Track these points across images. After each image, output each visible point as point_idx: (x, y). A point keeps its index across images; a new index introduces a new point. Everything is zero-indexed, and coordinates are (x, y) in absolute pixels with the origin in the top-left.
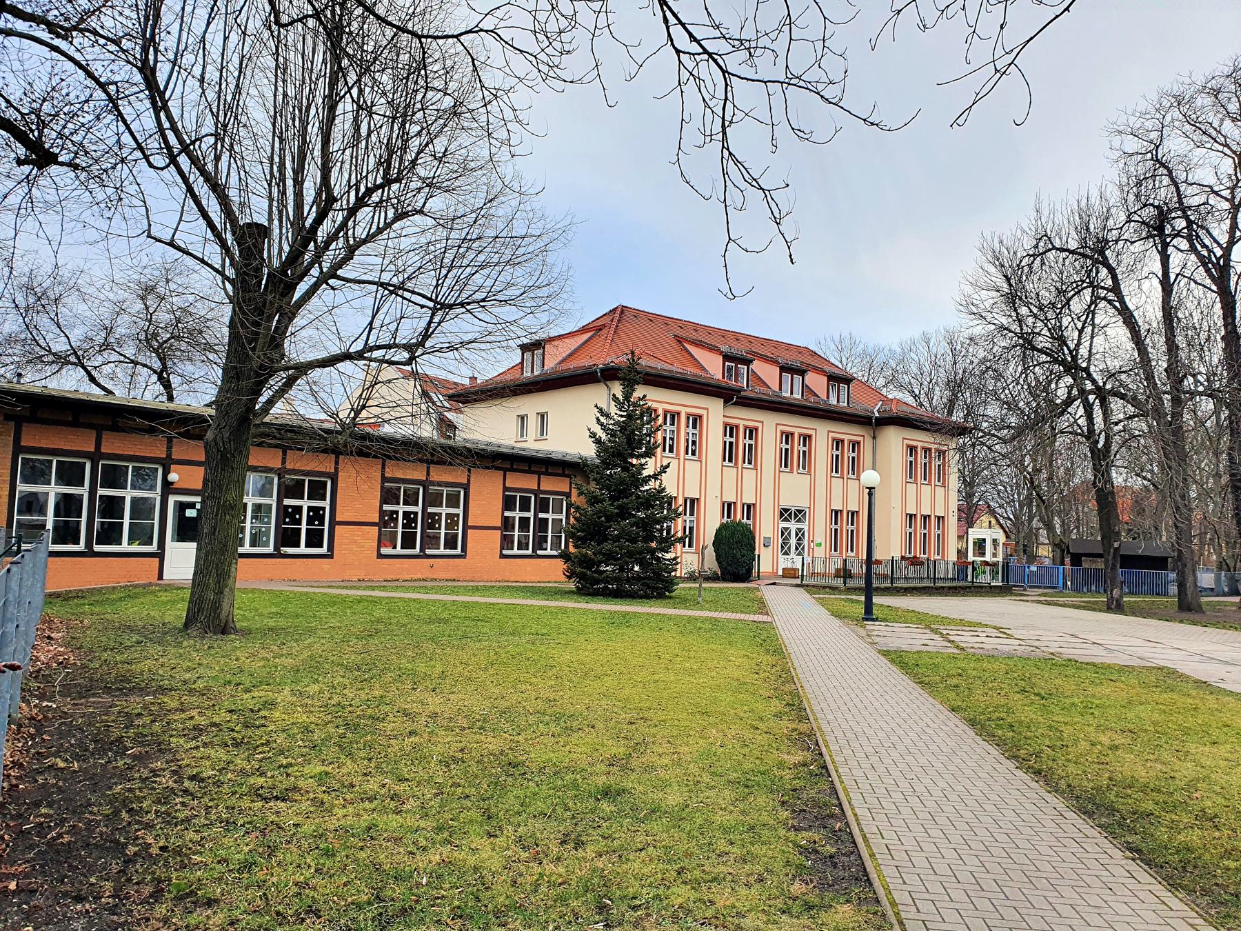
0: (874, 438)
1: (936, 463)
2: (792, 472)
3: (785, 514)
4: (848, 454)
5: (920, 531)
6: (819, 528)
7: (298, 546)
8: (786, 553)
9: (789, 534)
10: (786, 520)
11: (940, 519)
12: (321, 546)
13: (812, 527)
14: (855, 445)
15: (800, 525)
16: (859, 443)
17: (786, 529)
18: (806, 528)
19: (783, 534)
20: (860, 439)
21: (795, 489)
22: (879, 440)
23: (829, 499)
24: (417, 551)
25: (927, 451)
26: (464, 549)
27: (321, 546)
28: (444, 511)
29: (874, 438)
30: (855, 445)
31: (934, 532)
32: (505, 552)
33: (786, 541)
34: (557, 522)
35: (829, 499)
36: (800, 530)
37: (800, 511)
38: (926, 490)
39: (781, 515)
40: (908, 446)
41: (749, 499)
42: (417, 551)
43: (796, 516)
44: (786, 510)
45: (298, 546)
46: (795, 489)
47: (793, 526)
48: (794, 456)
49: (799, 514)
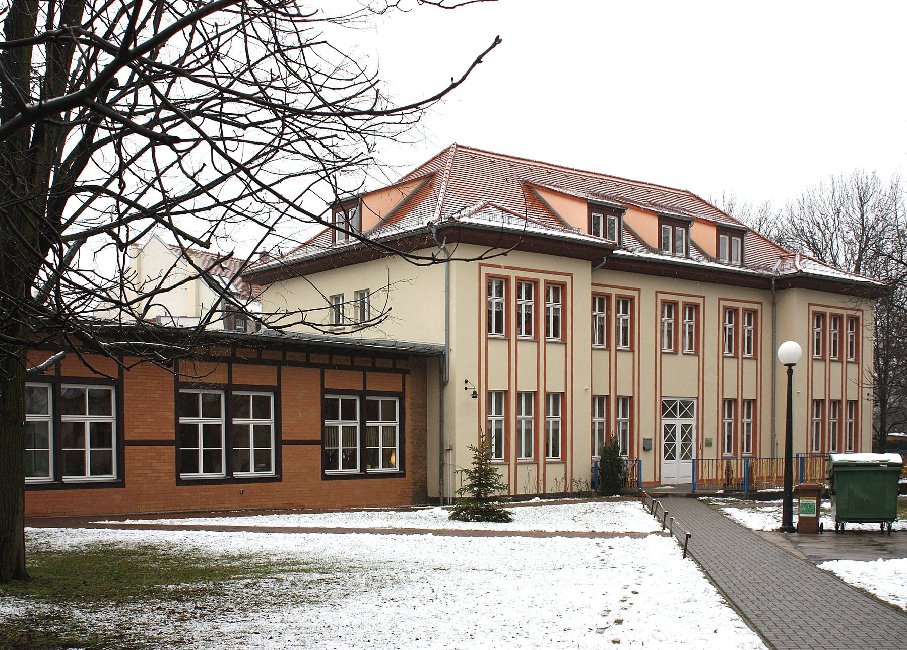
0: (774, 304)
1: (847, 333)
2: (676, 353)
3: (668, 408)
4: (745, 327)
5: (830, 419)
6: (710, 421)
7: (83, 473)
8: (670, 457)
9: (674, 432)
10: (670, 415)
11: (853, 404)
12: (111, 473)
13: (701, 422)
14: (752, 314)
15: (686, 421)
16: (755, 312)
17: (669, 426)
18: (694, 424)
19: (666, 433)
20: (756, 306)
21: (680, 377)
22: (778, 307)
23: (720, 386)
24: (223, 474)
25: (837, 318)
26: (279, 469)
27: (111, 473)
28: (380, 424)
29: (774, 304)
30: (752, 314)
31: (846, 420)
32: (328, 472)
33: (671, 439)
34: (389, 431)
35: (720, 386)
36: (686, 426)
37: (686, 403)
38: (836, 368)
39: (664, 408)
40: (815, 313)
41: (625, 390)
42: (223, 474)
43: (682, 409)
44: (670, 403)
45: (83, 473)
46: (680, 377)
47: (678, 422)
48: (680, 334)
49: (684, 408)
